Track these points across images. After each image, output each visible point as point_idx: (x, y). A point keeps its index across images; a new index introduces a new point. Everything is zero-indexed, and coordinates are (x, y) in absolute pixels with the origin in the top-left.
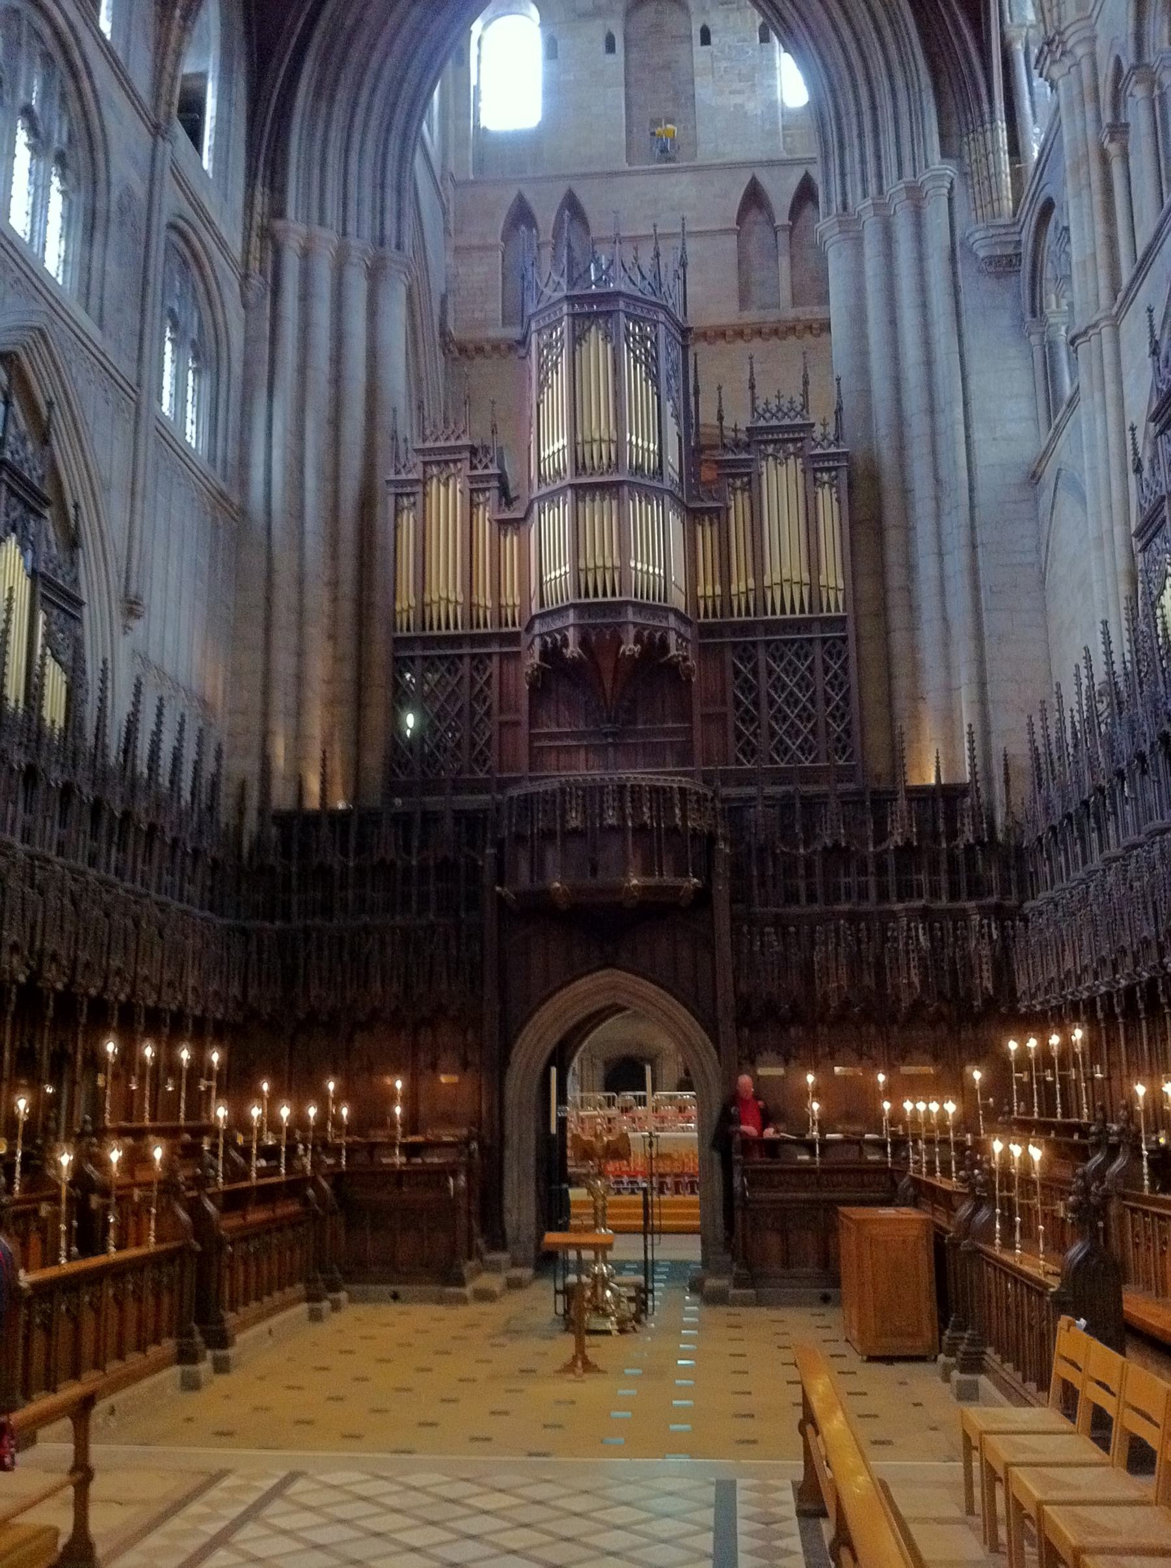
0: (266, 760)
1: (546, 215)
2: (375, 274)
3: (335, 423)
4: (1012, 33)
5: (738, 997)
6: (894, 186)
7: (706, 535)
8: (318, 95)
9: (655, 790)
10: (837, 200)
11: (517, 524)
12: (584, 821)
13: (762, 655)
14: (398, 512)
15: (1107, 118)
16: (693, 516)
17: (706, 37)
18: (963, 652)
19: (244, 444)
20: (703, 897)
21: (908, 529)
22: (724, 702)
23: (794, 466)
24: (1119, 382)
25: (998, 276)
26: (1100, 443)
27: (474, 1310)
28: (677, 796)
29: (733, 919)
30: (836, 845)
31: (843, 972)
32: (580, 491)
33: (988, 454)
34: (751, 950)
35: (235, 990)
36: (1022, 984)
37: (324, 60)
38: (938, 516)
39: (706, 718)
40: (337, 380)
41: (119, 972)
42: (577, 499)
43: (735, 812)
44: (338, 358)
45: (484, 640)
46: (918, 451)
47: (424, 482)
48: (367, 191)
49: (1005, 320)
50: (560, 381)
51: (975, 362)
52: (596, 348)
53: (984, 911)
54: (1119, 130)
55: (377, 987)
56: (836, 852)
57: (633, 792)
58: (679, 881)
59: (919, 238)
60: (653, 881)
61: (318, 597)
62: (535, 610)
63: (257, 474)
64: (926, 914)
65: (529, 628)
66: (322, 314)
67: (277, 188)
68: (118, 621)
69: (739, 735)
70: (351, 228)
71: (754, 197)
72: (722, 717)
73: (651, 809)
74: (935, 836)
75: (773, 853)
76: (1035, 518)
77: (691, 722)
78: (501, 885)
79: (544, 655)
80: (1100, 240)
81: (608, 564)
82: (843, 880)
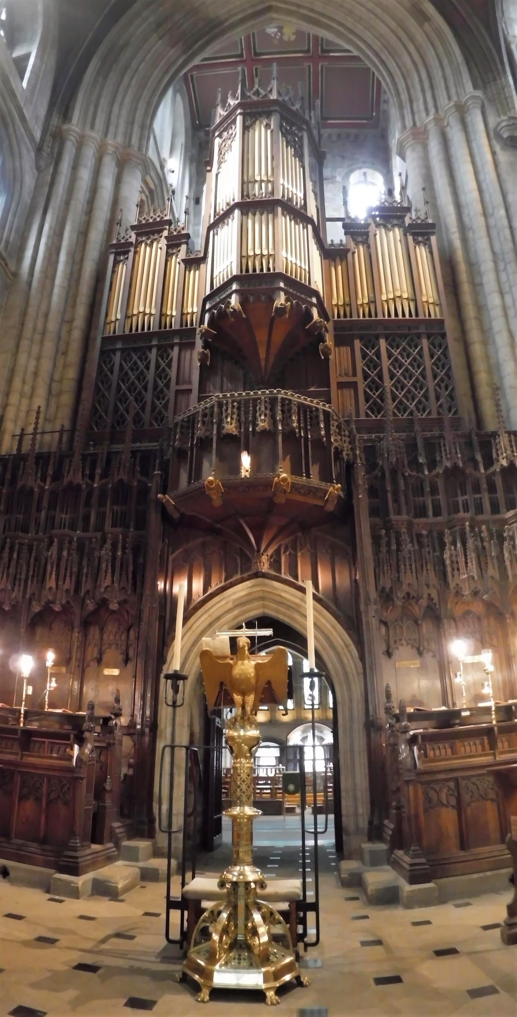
7: (337, 274)
9: (301, 406)
13: (383, 343)
22: (354, 374)
28: (322, 417)
30: (455, 466)
34: (389, 551)
38: (497, 271)
55: (51, 583)
57: (283, 406)
58: (323, 485)
69: (367, 398)
72: (354, 385)
73: (299, 421)
75: (403, 475)
77: (329, 386)
78: (164, 493)
82: (460, 499)
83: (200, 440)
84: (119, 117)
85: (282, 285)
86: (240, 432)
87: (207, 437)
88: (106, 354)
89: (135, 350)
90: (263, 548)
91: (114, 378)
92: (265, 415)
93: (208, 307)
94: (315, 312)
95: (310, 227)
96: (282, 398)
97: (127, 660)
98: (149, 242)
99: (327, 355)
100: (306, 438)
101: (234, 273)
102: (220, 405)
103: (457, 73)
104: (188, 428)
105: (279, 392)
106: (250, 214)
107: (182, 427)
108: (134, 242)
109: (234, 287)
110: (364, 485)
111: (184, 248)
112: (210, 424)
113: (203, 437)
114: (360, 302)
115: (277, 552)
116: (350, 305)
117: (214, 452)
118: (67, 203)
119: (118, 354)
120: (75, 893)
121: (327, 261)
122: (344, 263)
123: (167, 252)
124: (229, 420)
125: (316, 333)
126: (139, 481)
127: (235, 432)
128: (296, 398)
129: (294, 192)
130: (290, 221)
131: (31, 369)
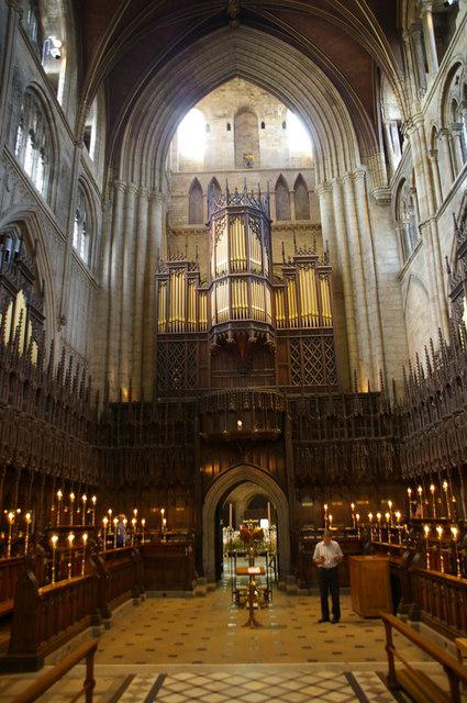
0: (107, 383)
1: (205, 186)
2: (151, 200)
3: (135, 254)
4: (385, 122)
5: (296, 476)
6: (343, 173)
7: (279, 298)
8: (131, 137)
10: (322, 178)
11: (207, 292)
13: (301, 343)
14: (160, 286)
15: (429, 148)
16: (274, 290)
17: (263, 126)
18: (376, 342)
19: (101, 262)
20: (282, 437)
21: (353, 296)
23: (311, 272)
24: (438, 242)
25: (383, 206)
26: (432, 264)
27: (197, 601)
29: (293, 445)
30: (332, 416)
31: (337, 465)
32: (233, 279)
33: (382, 269)
35: (96, 474)
36: (404, 468)
37: (133, 125)
39: (280, 367)
40: (136, 238)
41: (57, 464)
42: (231, 281)
43: (293, 403)
44: (137, 230)
45: (193, 336)
46: (357, 267)
48: (149, 171)
49: (386, 222)
50: (224, 238)
51: (376, 236)
52: (238, 227)
53: (387, 440)
54: (434, 152)
56: (332, 419)
59: (354, 193)
60: (263, 430)
61: (127, 320)
62: (214, 324)
63: (106, 272)
64: (366, 442)
65: (212, 331)
66: (131, 214)
67: (116, 169)
68: (57, 326)
70: (143, 183)
71: (281, 181)
72: (286, 367)
74: (369, 412)
76: (400, 293)
79: (218, 341)
80: (429, 191)
82: (334, 430)
84: (146, 166)
88: (160, 345)
97: (187, 504)
103: (351, 149)
118: (124, 234)
120: (192, 597)
131: (117, 348)
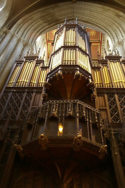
9: (86, 108)
12: (58, 114)
13: (116, 96)
14: (17, 66)
22: (106, 106)
47: (26, 62)
81: (72, 60)
83: (39, 118)
85: (78, 69)
86: (58, 116)
87: (43, 118)
89: (18, 92)
90: (65, 178)
91: (7, 101)
92: (71, 109)
93: (49, 76)
94: (90, 80)
95: (88, 57)
96: (79, 104)
98: (29, 62)
99: (94, 99)
100: (89, 123)
101: (60, 64)
102: (50, 105)
104: (35, 116)
105: (77, 101)
106: (67, 50)
107: (32, 115)
108: (24, 61)
109: (60, 68)
110: (117, 148)
111: (42, 64)
112: (45, 113)
113: (41, 118)
114: (106, 83)
115: (72, 182)
116: (102, 83)
117: (45, 124)
119: (11, 93)
121: (93, 70)
122: (99, 71)
123: (36, 65)
124: (54, 110)
125: (91, 88)
126: (8, 141)
127: (56, 116)
128: (85, 105)
129: (82, 47)
130: (81, 53)
